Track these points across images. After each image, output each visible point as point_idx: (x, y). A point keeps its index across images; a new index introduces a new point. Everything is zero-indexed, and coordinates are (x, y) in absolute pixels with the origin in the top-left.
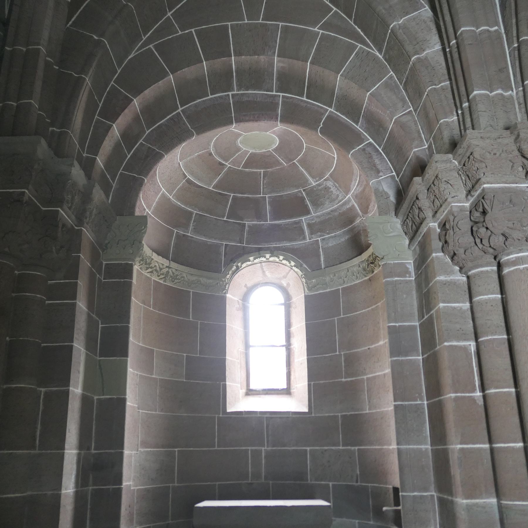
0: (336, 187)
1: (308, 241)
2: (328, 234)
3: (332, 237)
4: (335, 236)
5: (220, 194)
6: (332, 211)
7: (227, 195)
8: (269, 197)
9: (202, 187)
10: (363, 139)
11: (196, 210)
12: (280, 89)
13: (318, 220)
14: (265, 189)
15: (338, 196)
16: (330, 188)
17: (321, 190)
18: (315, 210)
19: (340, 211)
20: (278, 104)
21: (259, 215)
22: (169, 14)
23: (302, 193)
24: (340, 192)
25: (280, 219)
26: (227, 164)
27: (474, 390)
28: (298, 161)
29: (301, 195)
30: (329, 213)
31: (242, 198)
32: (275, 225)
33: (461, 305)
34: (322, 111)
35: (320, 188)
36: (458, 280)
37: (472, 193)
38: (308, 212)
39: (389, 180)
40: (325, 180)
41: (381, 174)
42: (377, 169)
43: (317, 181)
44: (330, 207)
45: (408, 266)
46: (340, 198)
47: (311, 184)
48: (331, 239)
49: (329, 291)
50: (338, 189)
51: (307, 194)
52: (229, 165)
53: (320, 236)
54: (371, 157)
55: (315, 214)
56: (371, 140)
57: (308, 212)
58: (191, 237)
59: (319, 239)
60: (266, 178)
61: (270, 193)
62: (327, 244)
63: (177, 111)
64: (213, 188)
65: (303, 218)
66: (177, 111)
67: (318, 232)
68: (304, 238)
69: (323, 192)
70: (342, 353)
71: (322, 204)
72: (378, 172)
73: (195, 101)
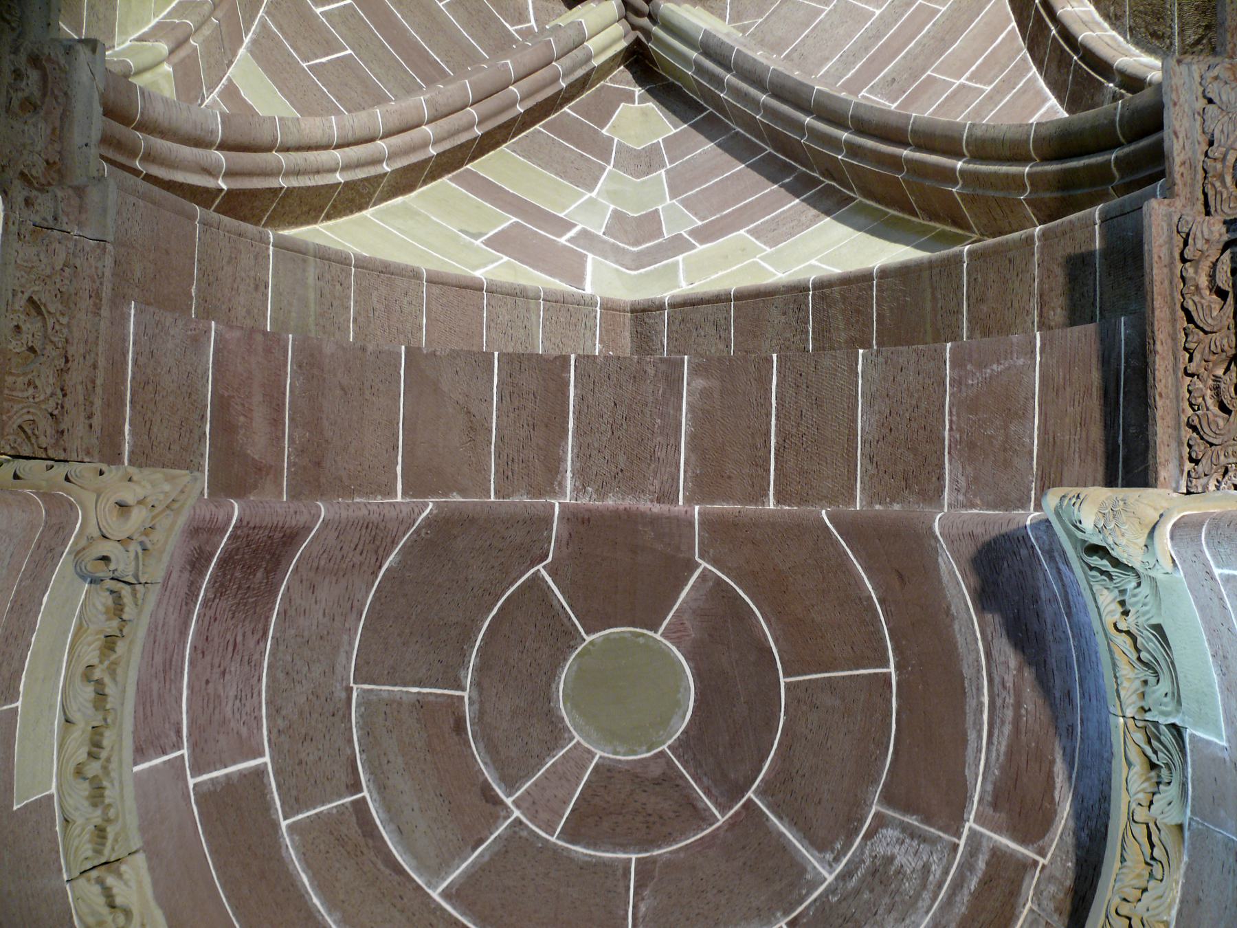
15: (926, 869)
16: (892, 859)
17: (857, 892)
40: (868, 836)
43: (837, 859)
46: (936, 869)
50: (923, 838)
60: (646, 893)
64: (446, 894)
69: (866, 896)
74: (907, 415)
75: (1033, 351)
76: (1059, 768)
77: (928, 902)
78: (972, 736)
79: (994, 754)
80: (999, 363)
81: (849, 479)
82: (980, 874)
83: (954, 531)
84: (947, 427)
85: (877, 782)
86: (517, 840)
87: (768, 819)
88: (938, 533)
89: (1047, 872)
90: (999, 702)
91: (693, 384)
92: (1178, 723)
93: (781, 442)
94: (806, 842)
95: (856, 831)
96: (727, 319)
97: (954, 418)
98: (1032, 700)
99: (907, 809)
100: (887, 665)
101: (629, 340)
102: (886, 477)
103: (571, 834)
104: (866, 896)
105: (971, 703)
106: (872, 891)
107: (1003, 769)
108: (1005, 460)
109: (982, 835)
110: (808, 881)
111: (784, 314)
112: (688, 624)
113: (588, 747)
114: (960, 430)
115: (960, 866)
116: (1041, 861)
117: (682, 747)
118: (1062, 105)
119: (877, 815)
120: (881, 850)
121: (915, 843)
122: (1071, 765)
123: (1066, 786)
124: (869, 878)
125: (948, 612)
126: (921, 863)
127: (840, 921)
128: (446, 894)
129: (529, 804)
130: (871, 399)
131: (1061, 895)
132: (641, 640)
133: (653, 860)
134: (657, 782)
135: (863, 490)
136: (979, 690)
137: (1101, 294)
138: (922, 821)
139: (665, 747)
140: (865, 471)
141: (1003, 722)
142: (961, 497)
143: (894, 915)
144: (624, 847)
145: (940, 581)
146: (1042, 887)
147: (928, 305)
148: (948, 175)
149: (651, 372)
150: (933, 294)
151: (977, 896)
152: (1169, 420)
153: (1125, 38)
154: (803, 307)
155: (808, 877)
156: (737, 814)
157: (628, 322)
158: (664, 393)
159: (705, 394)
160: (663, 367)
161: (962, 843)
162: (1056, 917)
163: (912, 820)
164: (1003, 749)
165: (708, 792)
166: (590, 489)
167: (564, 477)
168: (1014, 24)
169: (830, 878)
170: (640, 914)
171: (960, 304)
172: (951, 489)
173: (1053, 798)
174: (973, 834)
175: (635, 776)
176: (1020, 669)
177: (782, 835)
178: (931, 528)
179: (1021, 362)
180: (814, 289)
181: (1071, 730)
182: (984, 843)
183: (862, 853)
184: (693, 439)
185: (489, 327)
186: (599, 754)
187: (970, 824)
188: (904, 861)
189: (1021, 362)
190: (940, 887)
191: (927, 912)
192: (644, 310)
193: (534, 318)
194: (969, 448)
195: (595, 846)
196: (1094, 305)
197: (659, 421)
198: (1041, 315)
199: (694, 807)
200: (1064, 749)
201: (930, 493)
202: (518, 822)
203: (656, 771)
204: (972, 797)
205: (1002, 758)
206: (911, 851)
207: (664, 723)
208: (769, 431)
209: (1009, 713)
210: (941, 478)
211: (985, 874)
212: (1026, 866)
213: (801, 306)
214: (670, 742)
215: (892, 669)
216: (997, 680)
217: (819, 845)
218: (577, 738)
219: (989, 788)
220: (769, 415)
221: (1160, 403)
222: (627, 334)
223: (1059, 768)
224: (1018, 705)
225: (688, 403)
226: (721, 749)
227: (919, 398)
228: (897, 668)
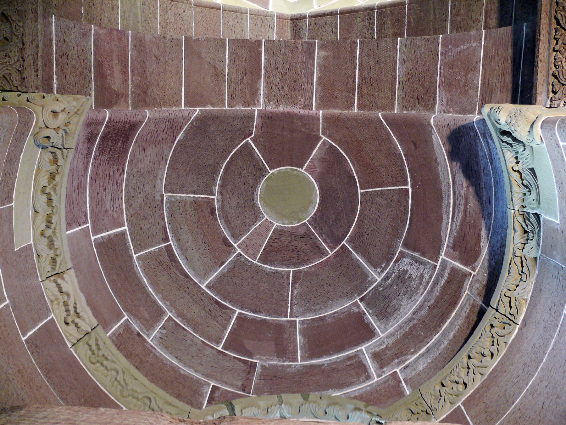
1: (376, 379)
2: (413, 353)
3: (421, 356)
4: (428, 350)
5: (217, 302)
6: (414, 313)
7: (229, 308)
8: (302, 322)
9: (188, 277)
11: (171, 312)
14: (294, 307)
15: (422, 276)
16: (407, 271)
17: (391, 285)
19: (429, 304)
21: (283, 350)
23: (359, 307)
24: (425, 264)
25: (319, 356)
29: (356, 310)
30: (410, 320)
31: (253, 320)
32: (312, 366)
35: (389, 282)
38: (370, 333)
44: (411, 307)
46: (426, 276)
48: (421, 359)
51: (368, 305)
53: (399, 363)
55: (384, 333)
57: (370, 333)
61: (302, 314)
62: (415, 370)
64: (208, 287)
65: (363, 348)
67: (393, 359)
68: (368, 377)
71: (396, 309)
74: (420, 69)
75: (481, 39)
76: (483, 232)
77: (422, 290)
78: (445, 217)
79: (454, 226)
80: (464, 45)
81: (392, 99)
82: (446, 278)
83: (440, 124)
84: (439, 75)
86: (239, 263)
87: (352, 253)
88: (432, 124)
89: (475, 278)
90: (457, 202)
91: (320, 54)
92: (538, 213)
93: (361, 81)
94: (369, 264)
95: (391, 259)
97: (442, 71)
98: (472, 202)
99: (414, 250)
100: (407, 185)
101: (289, 33)
102: (409, 98)
103: (264, 259)
105: (445, 203)
106: (397, 285)
107: (458, 232)
108: (465, 91)
109: (447, 261)
110: (369, 281)
111: (363, 21)
112: (317, 165)
113: (271, 220)
114: (445, 77)
115: (437, 275)
116: (473, 273)
117: (315, 220)
119: (401, 252)
120: (402, 268)
121: (417, 265)
123: (486, 240)
124: (397, 280)
126: (420, 273)
127: (383, 298)
128: (208, 287)
129: (245, 246)
130: (403, 61)
131: (481, 288)
132: (295, 173)
133: (300, 271)
135: (398, 104)
136: (449, 197)
137: (515, 12)
138: (421, 256)
139: (306, 221)
141: (459, 211)
142: (444, 108)
143: (407, 296)
145: (433, 147)
146: (473, 284)
147: (432, 17)
149: (300, 48)
150: (434, 12)
151: (444, 288)
152: (544, 73)
154: (372, 17)
155: (369, 279)
156: (338, 251)
157: (289, 25)
158: (306, 58)
159: (326, 58)
160: (306, 46)
161: (438, 265)
162: (478, 297)
163: (417, 255)
164: (458, 223)
166: (271, 103)
167: (259, 98)
169: (379, 280)
170: (294, 295)
171: (447, 17)
172: (439, 104)
173: (480, 246)
174: (444, 261)
175: (292, 233)
176: (468, 188)
177: (358, 260)
178: (429, 122)
179: (475, 44)
180: (378, 9)
181: (490, 214)
182: (448, 265)
183: (394, 269)
184: (320, 79)
185: (224, 27)
186: (276, 224)
187: (442, 257)
188: (412, 273)
189: (475, 44)
190: (428, 284)
191: (421, 295)
192: (297, 19)
193: (245, 23)
194: (448, 85)
195: (274, 265)
196: (511, 17)
197: (304, 71)
198: (485, 22)
199: (319, 248)
200: (486, 224)
201: (430, 106)
202: (240, 254)
203: (301, 232)
204: (443, 245)
205: (458, 227)
206: (416, 268)
207: (305, 210)
208: (355, 76)
209: (462, 208)
210: (435, 99)
211: (448, 278)
212: (466, 275)
213: (371, 17)
214: (308, 219)
216: (457, 192)
217: (375, 266)
218: (266, 217)
219: (452, 240)
220: (355, 68)
221: (540, 65)
222: (289, 30)
223: (483, 232)
224: (466, 204)
225: (317, 63)
226: (331, 222)
227: (426, 61)
228: (412, 186)
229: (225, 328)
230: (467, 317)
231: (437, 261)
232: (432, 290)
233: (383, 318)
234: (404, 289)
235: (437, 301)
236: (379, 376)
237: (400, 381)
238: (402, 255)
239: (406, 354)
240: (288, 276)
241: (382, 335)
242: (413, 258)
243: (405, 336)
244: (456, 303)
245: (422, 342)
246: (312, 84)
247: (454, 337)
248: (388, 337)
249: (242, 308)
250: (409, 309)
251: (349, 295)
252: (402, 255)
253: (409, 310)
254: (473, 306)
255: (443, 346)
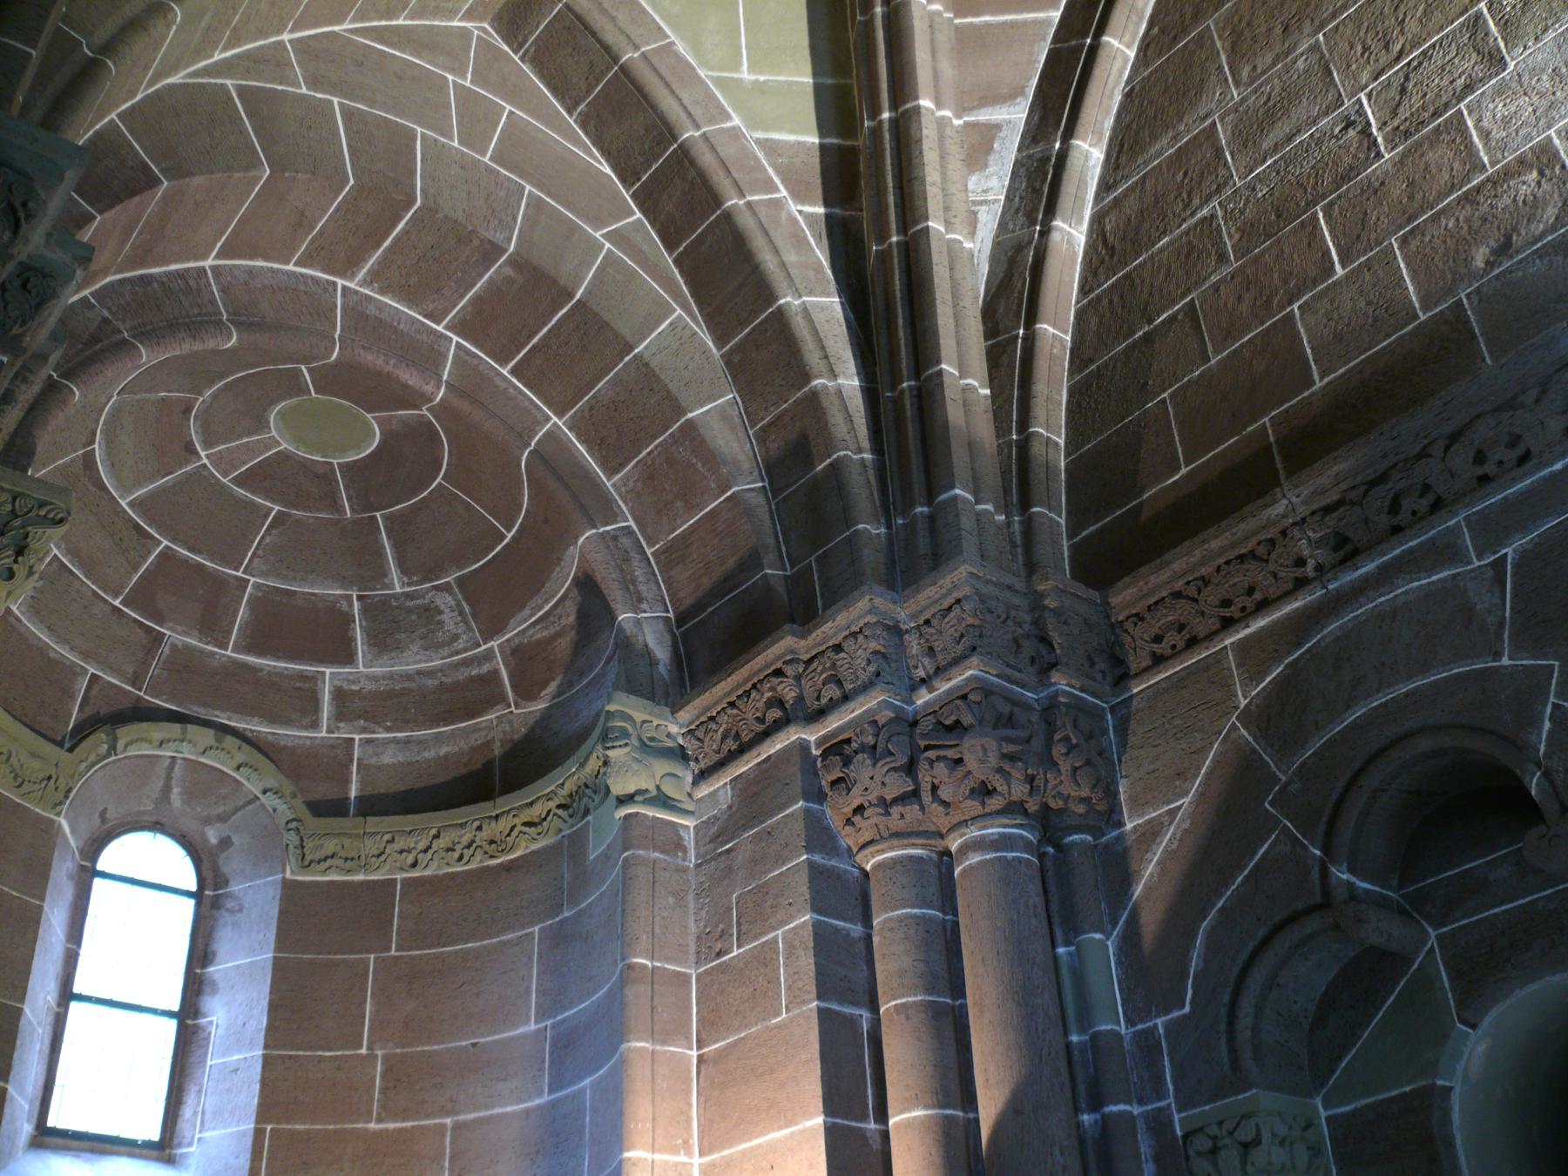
0: (461, 613)
1: (324, 734)
2: (388, 730)
3: (396, 741)
4: (407, 741)
5: (137, 526)
6: (419, 673)
7: (153, 538)
8: (257, 586)
9: (103, 488)
10: (616, 515)
11: (59, 548)
12: (460, 327)
13: (370, 686)
14: (256, 561)
15: (456, 637)
16: (442, 612)
17: (410, 611)
18: (370, 657)
20: (445, 357)
21: (213, 626)
22: (286, 37)
23: (351, 605)
24: (470, 629)
25: (261, 653)
26: (203, 454)
27: (863, 1117)
28: (384, 517)
29: (345, 607)
30: (408, 677)
31: (185, 562)
32: (245, 665)
33: (848, 925)
34: (539, 416)
36: (846, 871)
37: (936, 683)
38: (348, 658)
39: (661, 626)
40: (436, 588)
41: (644, 606)
42: (638, 592)
43: (409, 584)
44: (420, 662)
45: (682, 832)
46: (460, 644)
47: (391, 586)
49: (363, 883)
50: (466, 622)
51: (365, 611)
52: (205, 461)
53: (364, 730)
54: (627, 560)
55: (367, 668)
56: (632, 523)
57: (348, 658)
58: (17, 619)
59: (357, 737)
61: (264, 575)
63: (200, 264)
65: (328, 671)
66: (200, 264)
68: (315, 725)
69: (414, 617)
70: (379, 1053)
71: (399, 648)
72: (641, 600)
73: (251, 258)
75: (724, 492)
76: (553, 687)
78: (527, 612)
85: (461, 568)
86: (201, 475)
96: (603, 74)
98: (565, 644)
99: (467, 599)
100: (509, 531)
103: (238, 481)
104: (414, 617)
113: (277, 437)
118: (1055, 40)
120: (438, 602)
122: (559, 693)
125: (559, 559)
128: (131, 504)
129: (217, 460)
130: (616, 381)
133: (290, 515)
134: (317, 475)
136: (547, 601)
140: (581, 410)
141: (546, 628)
144: (274, 501)
148: (875, 112)
149: (476, 243)
151: (472, 679)
153: (1127, 83)
159: (508, 280)
164: (538, 636)
165: (349, 500)
168: (1056, 15)
169: (398, 590)
175: (305, 467)
176: (572, 627)
178: (577, 538)
179: (713, 485)
181: (571, 685)
186: (285, 445)
187: (494, 644)
189: (713, 485)
190: (457, 653)
194: (649, 474)
195: (253, 493)
196: (788, 486)
198: (770, 424)
202: (204, 466)
203: (321, 471)
207: (343, 450)
208: (536, 333)
209: (552, 631)
210: (622, 466)
212: (502, 699)
215: (510, 536)
217: (404, 570)
218: (274, 433)
220: (545, 324)
223: (553, 687)
224: (558, 635)
229: (135, 570)
230: (474, 750)
231: (485, 641)
232: (457, 665)
233: (375, 645)
234: (424, 630)
235: (456, 687)
236: (330, 731)
237: (352, 760)
238: (446, 588)
239: (378, 723)
240: (266, 516)
241: (361, 669)
242: (459, 605)
243: (391, 694)
244: (473, 717)
245: (403, 723)
246: (462, 297)
247: (446, 757)
248: (368, 677)
249: (173, 541)
250: (413, 661)
251: (345, 582)
252: (446, 588)
253: (415, 663)
254: (487, 744)
255: (426, 754)
